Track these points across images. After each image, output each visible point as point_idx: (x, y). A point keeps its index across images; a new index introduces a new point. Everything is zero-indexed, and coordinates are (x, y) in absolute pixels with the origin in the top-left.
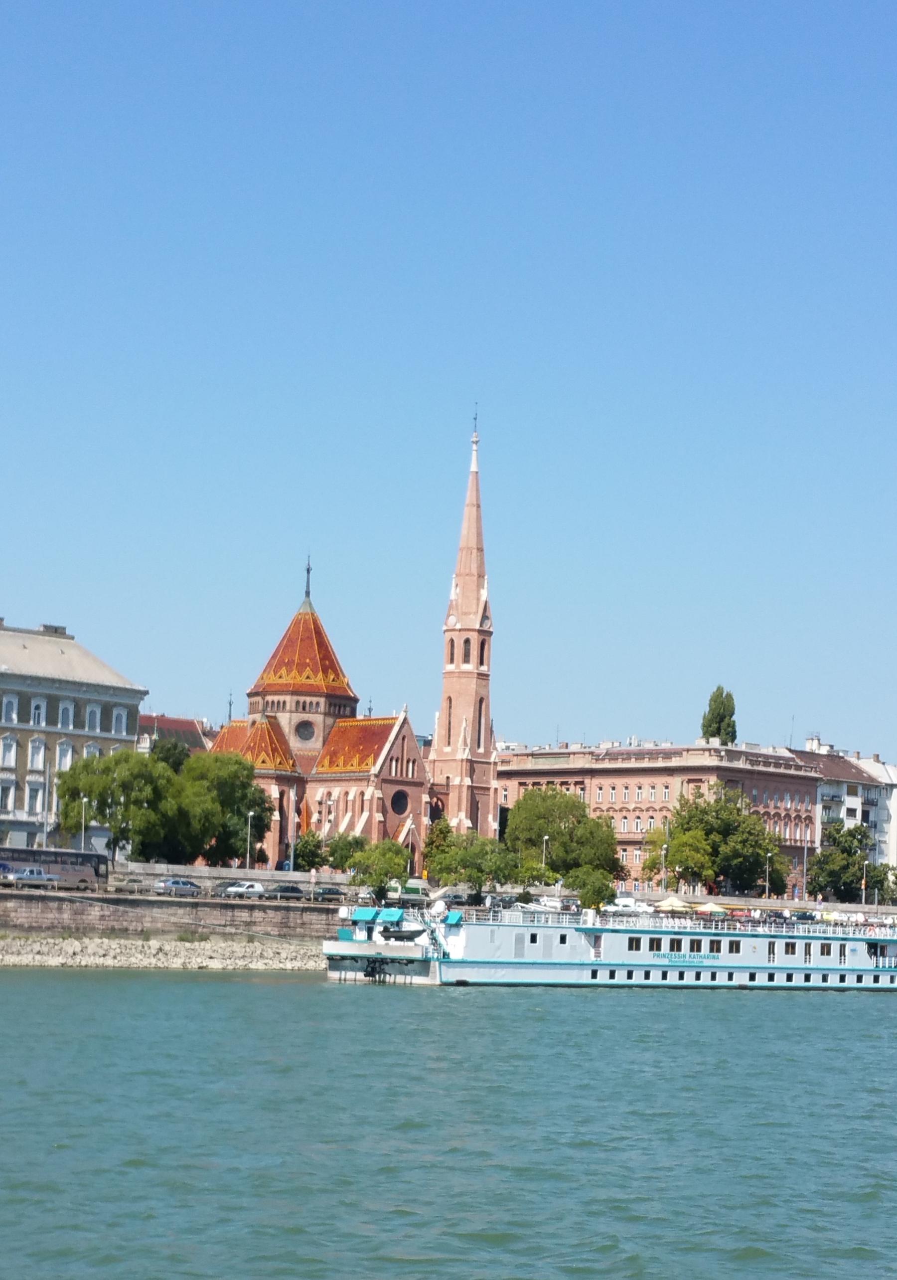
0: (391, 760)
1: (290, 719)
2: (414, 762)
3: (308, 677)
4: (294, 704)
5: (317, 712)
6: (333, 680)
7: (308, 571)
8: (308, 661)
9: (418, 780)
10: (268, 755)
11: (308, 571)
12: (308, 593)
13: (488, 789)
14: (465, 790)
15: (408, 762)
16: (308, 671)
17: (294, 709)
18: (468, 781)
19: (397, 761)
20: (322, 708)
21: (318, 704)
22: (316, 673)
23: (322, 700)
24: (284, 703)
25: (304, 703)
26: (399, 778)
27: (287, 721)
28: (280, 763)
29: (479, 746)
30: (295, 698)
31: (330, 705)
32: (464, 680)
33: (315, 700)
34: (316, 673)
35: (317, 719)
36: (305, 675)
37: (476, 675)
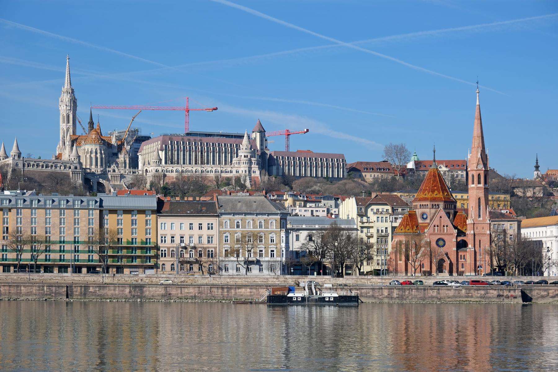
0: (435, 226)
2: (447, 226)
15: (444, 226)
16: (426, 192)
22: (429, 193)
29: (479, 216)
34: (429, 193)
35: (427, 211)
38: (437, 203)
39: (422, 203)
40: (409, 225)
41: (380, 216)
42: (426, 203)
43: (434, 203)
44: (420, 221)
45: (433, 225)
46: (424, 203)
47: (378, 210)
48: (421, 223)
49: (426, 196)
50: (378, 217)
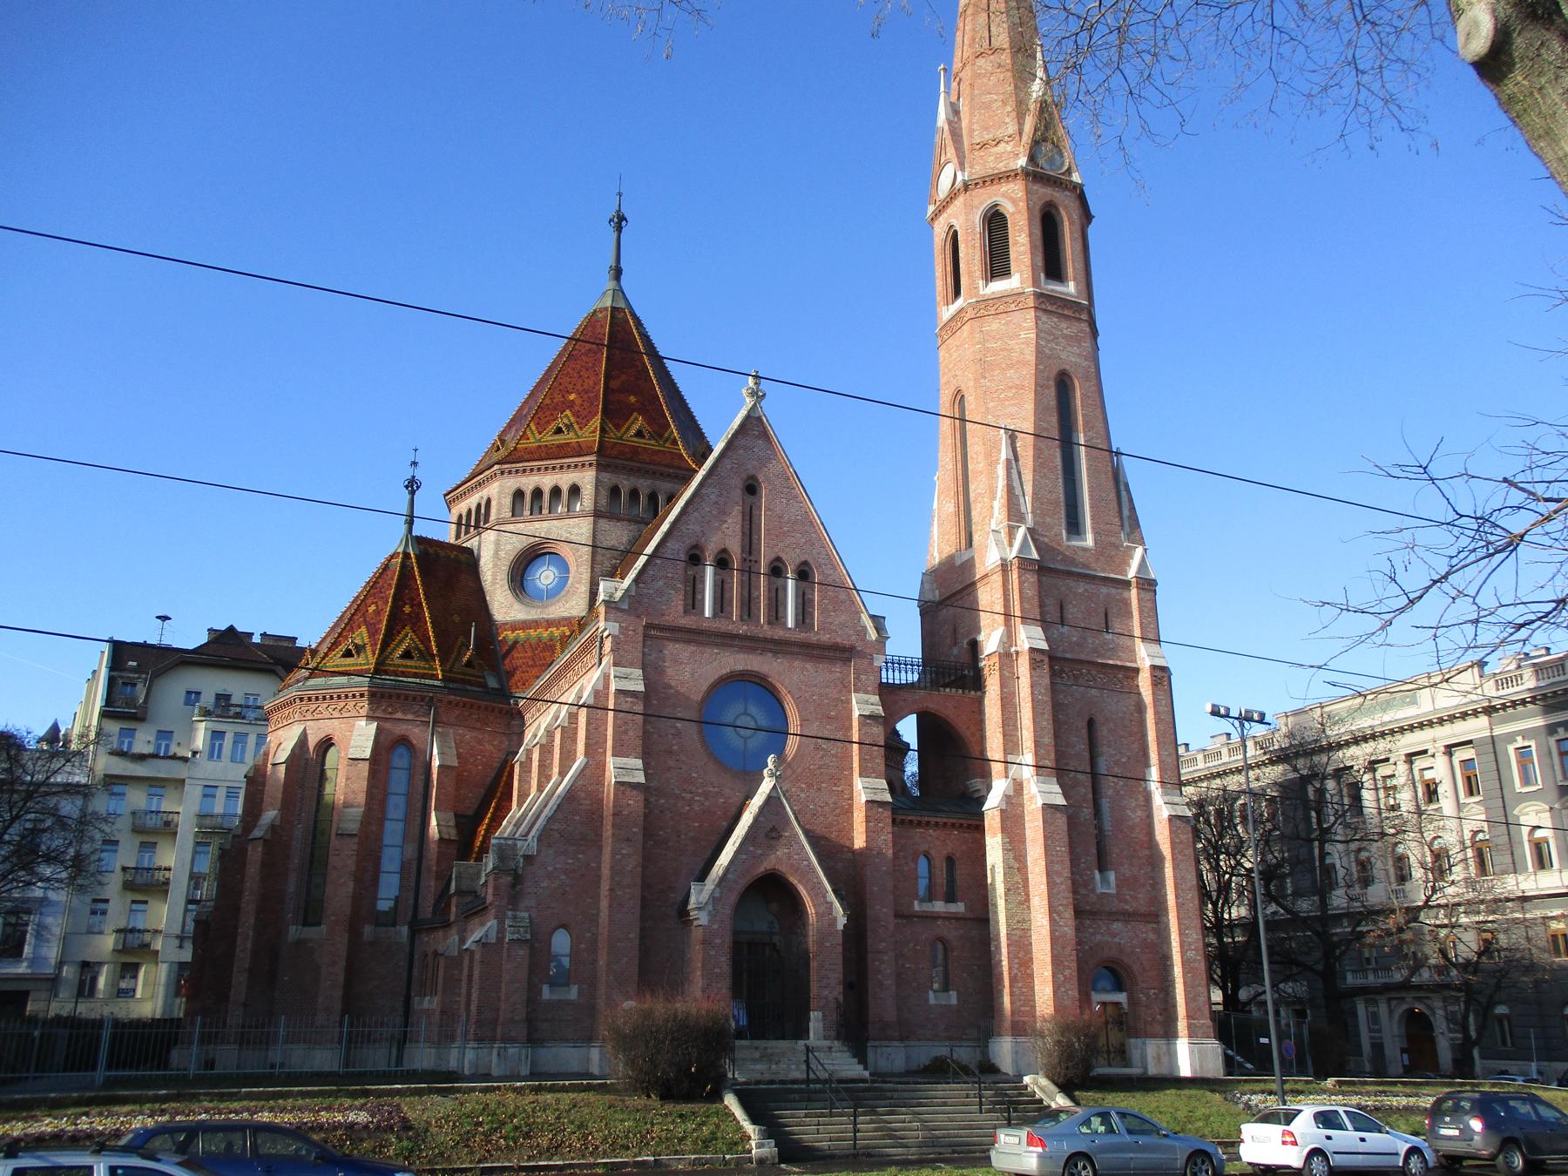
1: (497, 543)
2: (803, 574)
3: (559, 431)
4: (508, 501)
6: (639, 434)
7: (619, 221)
8: (572, 397)
9: (825, 638)
11: (619, 221)
12: (617, 273)
13: (1137, 670)
14: (1023, 668)
15: (777, 570)
18: (1029, 637)
19: (722, 563)
21: (575, 490)
22: (583, 420)
23: (587, 479)
25: (538, 493)
26: (734, 623)
27: (493, 553)
28: (407, 655)
29: (1074, 526)
30: (512, 483)
31: (615, 492)
32: (994, 325)
36: (553, 426)
37: (1031, 302)
38: (645, 486)
39: (528, 483)
40: (416, 621)
41: (230, 729)
42: (565, 480)
43: (625, 484)
44: (503, 606)
45: (678, 548)
46: (547, 481)
47: (223, 699)
48: (514, 626)
49: (567, 438)
50: (217, 735)
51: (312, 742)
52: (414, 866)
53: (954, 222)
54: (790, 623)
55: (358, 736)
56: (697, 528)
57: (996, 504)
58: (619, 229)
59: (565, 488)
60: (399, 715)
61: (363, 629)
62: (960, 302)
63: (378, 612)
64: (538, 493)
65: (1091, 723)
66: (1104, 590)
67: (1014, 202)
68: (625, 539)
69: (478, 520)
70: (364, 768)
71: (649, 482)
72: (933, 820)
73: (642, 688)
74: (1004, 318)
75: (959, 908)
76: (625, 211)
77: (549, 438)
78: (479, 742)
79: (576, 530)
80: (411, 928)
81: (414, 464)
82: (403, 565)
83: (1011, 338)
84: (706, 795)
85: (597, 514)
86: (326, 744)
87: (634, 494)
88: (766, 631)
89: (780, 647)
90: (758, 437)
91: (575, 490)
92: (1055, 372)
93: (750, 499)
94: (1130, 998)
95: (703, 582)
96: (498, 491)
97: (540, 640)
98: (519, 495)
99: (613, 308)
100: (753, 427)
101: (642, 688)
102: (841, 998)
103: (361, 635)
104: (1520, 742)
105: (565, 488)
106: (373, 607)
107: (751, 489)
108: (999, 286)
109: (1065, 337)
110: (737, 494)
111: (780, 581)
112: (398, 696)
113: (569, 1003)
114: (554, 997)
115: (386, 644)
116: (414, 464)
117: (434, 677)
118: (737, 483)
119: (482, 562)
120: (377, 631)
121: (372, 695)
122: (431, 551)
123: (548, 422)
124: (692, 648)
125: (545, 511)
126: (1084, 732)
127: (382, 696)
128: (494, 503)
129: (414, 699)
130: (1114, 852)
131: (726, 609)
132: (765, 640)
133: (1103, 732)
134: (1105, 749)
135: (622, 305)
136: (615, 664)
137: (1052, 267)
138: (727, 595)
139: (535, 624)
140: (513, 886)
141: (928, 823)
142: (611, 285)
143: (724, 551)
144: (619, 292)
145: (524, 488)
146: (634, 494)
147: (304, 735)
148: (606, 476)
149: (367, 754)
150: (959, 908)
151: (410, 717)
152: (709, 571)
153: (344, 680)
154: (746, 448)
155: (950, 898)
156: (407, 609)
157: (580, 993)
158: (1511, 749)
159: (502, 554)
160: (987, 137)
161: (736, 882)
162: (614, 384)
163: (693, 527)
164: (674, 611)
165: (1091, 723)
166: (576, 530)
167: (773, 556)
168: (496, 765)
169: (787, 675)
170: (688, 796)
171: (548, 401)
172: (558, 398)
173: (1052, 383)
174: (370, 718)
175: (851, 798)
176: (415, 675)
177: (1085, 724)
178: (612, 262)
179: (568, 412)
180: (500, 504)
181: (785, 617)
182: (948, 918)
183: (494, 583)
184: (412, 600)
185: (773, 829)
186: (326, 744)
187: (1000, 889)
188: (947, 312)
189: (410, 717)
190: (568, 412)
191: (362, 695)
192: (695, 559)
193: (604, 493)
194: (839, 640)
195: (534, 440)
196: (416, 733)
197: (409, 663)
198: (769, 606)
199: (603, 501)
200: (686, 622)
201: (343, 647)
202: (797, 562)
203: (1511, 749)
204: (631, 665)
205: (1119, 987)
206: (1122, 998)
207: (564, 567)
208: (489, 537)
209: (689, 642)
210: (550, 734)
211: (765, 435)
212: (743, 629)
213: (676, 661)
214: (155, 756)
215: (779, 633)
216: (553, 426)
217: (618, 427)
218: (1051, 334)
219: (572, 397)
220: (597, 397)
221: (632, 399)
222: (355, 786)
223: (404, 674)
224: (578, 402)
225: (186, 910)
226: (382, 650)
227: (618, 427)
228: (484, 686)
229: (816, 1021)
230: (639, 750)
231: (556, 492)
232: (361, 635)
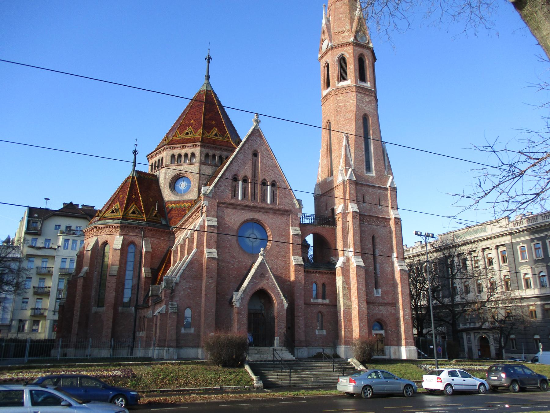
0: (235, 179)
1: (166, 173)
2: (273, 185)
3: (187, 134)
4: (169, 158)
5: (191, 163)
6: (216, 135)
7: (209, 59)
8: (192, 121)
9: (281, 207)
10: (121, 205)
11: (209, 59)
12: (208, 77)
13: (390, 219)
15: (264, 183)
17: (169, 163)
18: (352, 207)
19: (245, 181)
20: (197, 158)
21: (193, 155)
22: (196, 130)
23: (197, 151)
24: (162, 158)
25: (180, 156)
26: (249, 202)
27: (164, 176)
28: (134, 212)
29: (368, 169)
30: (171, 152)
31: (207, 155)
32: (341, 97)
33: (189, 151)
36: (185, 132)
37: (354, 89)
38: (218, 153)
39: (176, 152)
40: (137, 200)
41: (71, 238)
42: (189, 151)
43: (211, 152)
44: (168, 196)
45: (229, 175)
46: (183, 151)
47: (68, 228)
48: (172, 202)
49: (190, 136)
50: (66, 240)
51: (100, 243)
52: (137, 286)
53: (328, 60)
54: (269, 202)
55: (117, 241)
56: (236, 168)
57: (341, 161)
58: (209, 62)
59: (189, 154)
60: (131, 234)
61: (118, 203)
62: (329, 89)
63: (123, 198)
64: (180, 156)
65: (373, 237)
66: (379, 191)
67: (349, 53)
68: (211, 172)
69: (159, 165)
70: (119, 252)
71: (219, 152)
72: (318, 271)
73: (216, 224)
74: (345, 95)
75: (327, 301)
76: (211, 55)
77: (184, 136)
78: (159, 243)
79: (193, 169)
80: (135, 308)
81: (136, 145)
82: (132, 181)
83: (347, 102)
84: (239, 262)
85: (201, 163)
86: (105, 244)
87: (214, 156)
88: (261, 205)
89: (265, 210)
90: (257, 136)
91: (193, 155)
92: (362, 114)
93: (255, 158)
94: (386, 333)
95: (238, 187)
96: (166, 155)
97: (180, 207)
98: (173, 156)
99: (207, 90)
100: (256, 133)
101: (216, 224)
102: (285, 332)
103: (117, 205)
104: (521, 245)
105: (189, 154)
106: (121, 196)
107: (255, 154)
108: (343, 83)
109: (366, 102)
110: (250, 156)
111: (265, 187)
112: (131, 227)
113: (191, 334)
114: (185, 332)
115: (126, 209)
116: (136, 145)
117: (143, 220)
118: (250, 153)
119: (160, 180)
120: (123, 204)
121: (121, 227)
122: (142, 176)
123: (184, 131)
124: (234, 210)
125: (183, 162)
126: (371, 240)
127: (125, 227)
128: (164, 159)
129: (136, 228)
130: (381, 282)
131: (246, 197)
132: (260, 208)
133: (377, 240)
134: (378, 246)
135: (210, 89)
136: (207, 216)
137: (362, 77)
138: (246, 192)
139: (179, 202)
140: (171, 293)
141: (316, 272)
142: (206, 82)
143: (246, 176)
144: (209, 84)
145: (175, 154)
146: (214, 156)
147: (97, 242)
148: (204, 150)
149: (120, 247)
150: (327, 301)
151: (135, 234)
152: (240, 183)
153: (111, 221)
154: (253, 140)
155: (324, 298)
156: (134, 196)
157: (195, 330)
158: (518, 247)
159: (167, 177)
160: (340, 30)
161: (249, 292)
162: (207, 117)
163: (234, 168)
164: (227, 196)
165: (373, 237)
166: (193, 169)
167: (263, 178)
168: (165, 251)
169: (267, 220)
170: (233, 262)
171: (183, 123)
172: (187, 122)
173: (361, 118)
174: (120, 234)
175: (290, 263)
176: (137, 220)
177: (371, 238)
178: (206, 73)
179: (190, 127)
180: (166, 159)
181: (267, 200)
182: (323, 305)
183: (164, 187)
184: (135, 193)
185: (262, 274)
186: (105, 244)
187: (341, 294)
188: (325, 93)
189: (135, 234)
190: (190, 127)
191: (118, 227)
192: (235, 179)
193: (203, 156)
194: (286, 208)
195: (179, 137)
196: (137, 240)
197: (134, 215)
198: (261, 196)
199: (203, 159)
200: (232, 201)
201: (111, 210)
202: (271, 180)
203: (518, 247)
204: (213, 216)
205: (382, 329)
206: (383, 332)
207: (189, 182)
208: (163, 171)
209: (233, 208)
210: (184, 240)
211: (260, 136)
212: (252, 204)
213: (229, 215)
214: (44, 248)
215: (265, 206)
216: (185, 132)
217: (208, 132)
218: (361, 101)
219: (192, 121)
220: (201, 121)
221: (213, 122)
222: (115, 259)
223: (132, 219)
224: (194, 123)
225: (56, 302)
226: (125, 211)
227: (208, 132)
228: (161, 223)
229: (277, 340)
230: (215, 246)
231: (186, 155)
232: (117, 205)
